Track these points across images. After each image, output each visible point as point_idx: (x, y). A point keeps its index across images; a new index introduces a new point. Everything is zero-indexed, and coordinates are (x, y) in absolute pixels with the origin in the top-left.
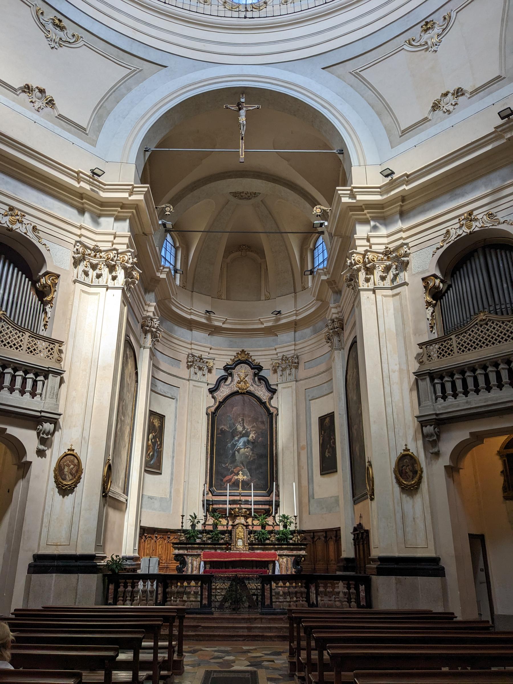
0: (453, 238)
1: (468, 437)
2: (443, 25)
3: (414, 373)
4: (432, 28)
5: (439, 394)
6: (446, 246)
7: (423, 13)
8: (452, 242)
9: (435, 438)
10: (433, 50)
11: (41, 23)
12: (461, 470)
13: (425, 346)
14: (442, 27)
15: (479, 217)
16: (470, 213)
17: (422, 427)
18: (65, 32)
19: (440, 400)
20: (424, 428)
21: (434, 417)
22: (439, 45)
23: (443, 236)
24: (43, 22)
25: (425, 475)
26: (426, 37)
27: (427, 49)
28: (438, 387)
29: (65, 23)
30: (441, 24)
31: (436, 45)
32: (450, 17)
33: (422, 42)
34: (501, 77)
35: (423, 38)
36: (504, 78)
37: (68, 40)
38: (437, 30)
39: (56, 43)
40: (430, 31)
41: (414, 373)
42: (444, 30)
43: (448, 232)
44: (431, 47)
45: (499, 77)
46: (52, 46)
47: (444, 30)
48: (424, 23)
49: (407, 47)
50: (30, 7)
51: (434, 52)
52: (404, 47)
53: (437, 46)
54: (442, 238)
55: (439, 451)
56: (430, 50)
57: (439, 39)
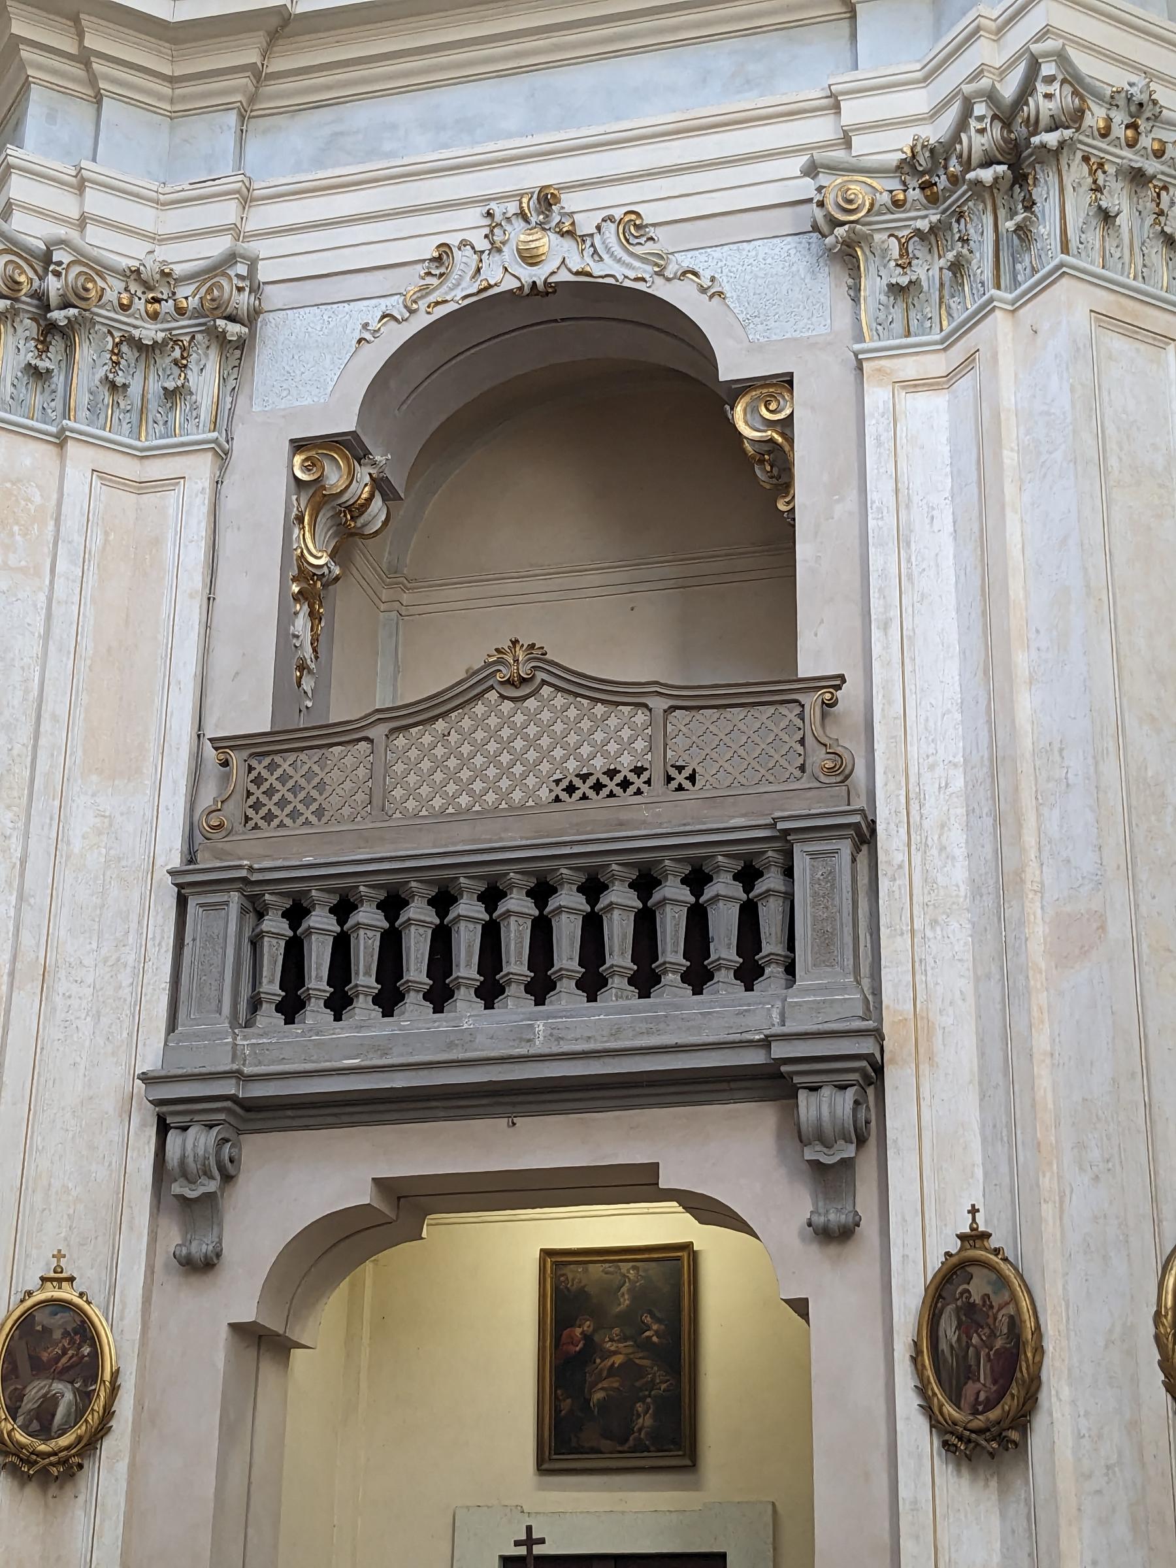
0: (459, 294)
1: (364, 1196)
3: (172, 873)
5: (271, 987)
6: (422, 321)
8: (453, 307)
9: (212, 1186)
12: (296, 1353)
13: (245, 754)
15: (586, 225)
16: (547, 199)
17: (163, 1128)
19: (269, 1018)
20: (173, 1138)
21: (228, 1088)
23: (421, 270)
25: (125, 1406)
28: (273, 953)
41: (172, 873)
43: (445, 250)
54: (411, 280)
55: (218, 1255)
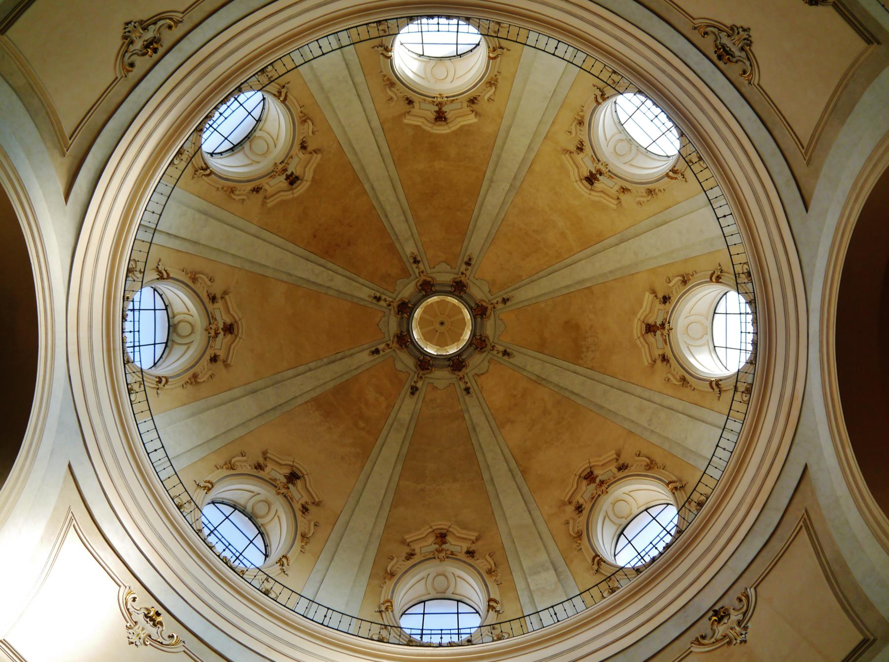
2: (742, 608)
4: (727, 614)
7: (707, 601)
10: (738, 641)
11: (128, 610)
14: (741, 611)
18: (161, 629)
22: (746, 633)
24: (131, 610)
26: (721, 629)
27: (729, 643)
29: (164, 618)
30: (738, 608)
31: (742, 634)
32: (747, 597)
33: (718, 636)
34: (868, 640)
35: (717, 632)
36: (875, 640)
37: (160, 640)
38: (735, 617)
39: (140, 638)
40: (725, 620)
42: (744, 614)
44: (736, 639)
45: (865, 641)
46: (131, 640)
47: (744, 614)
48: (711, 613)
49: (696, 649)
50: (120, 586)
51: (743, 644)
52: (692, 649)
53: (743, 636)
56: (734, 642)
57: (742, 626)
